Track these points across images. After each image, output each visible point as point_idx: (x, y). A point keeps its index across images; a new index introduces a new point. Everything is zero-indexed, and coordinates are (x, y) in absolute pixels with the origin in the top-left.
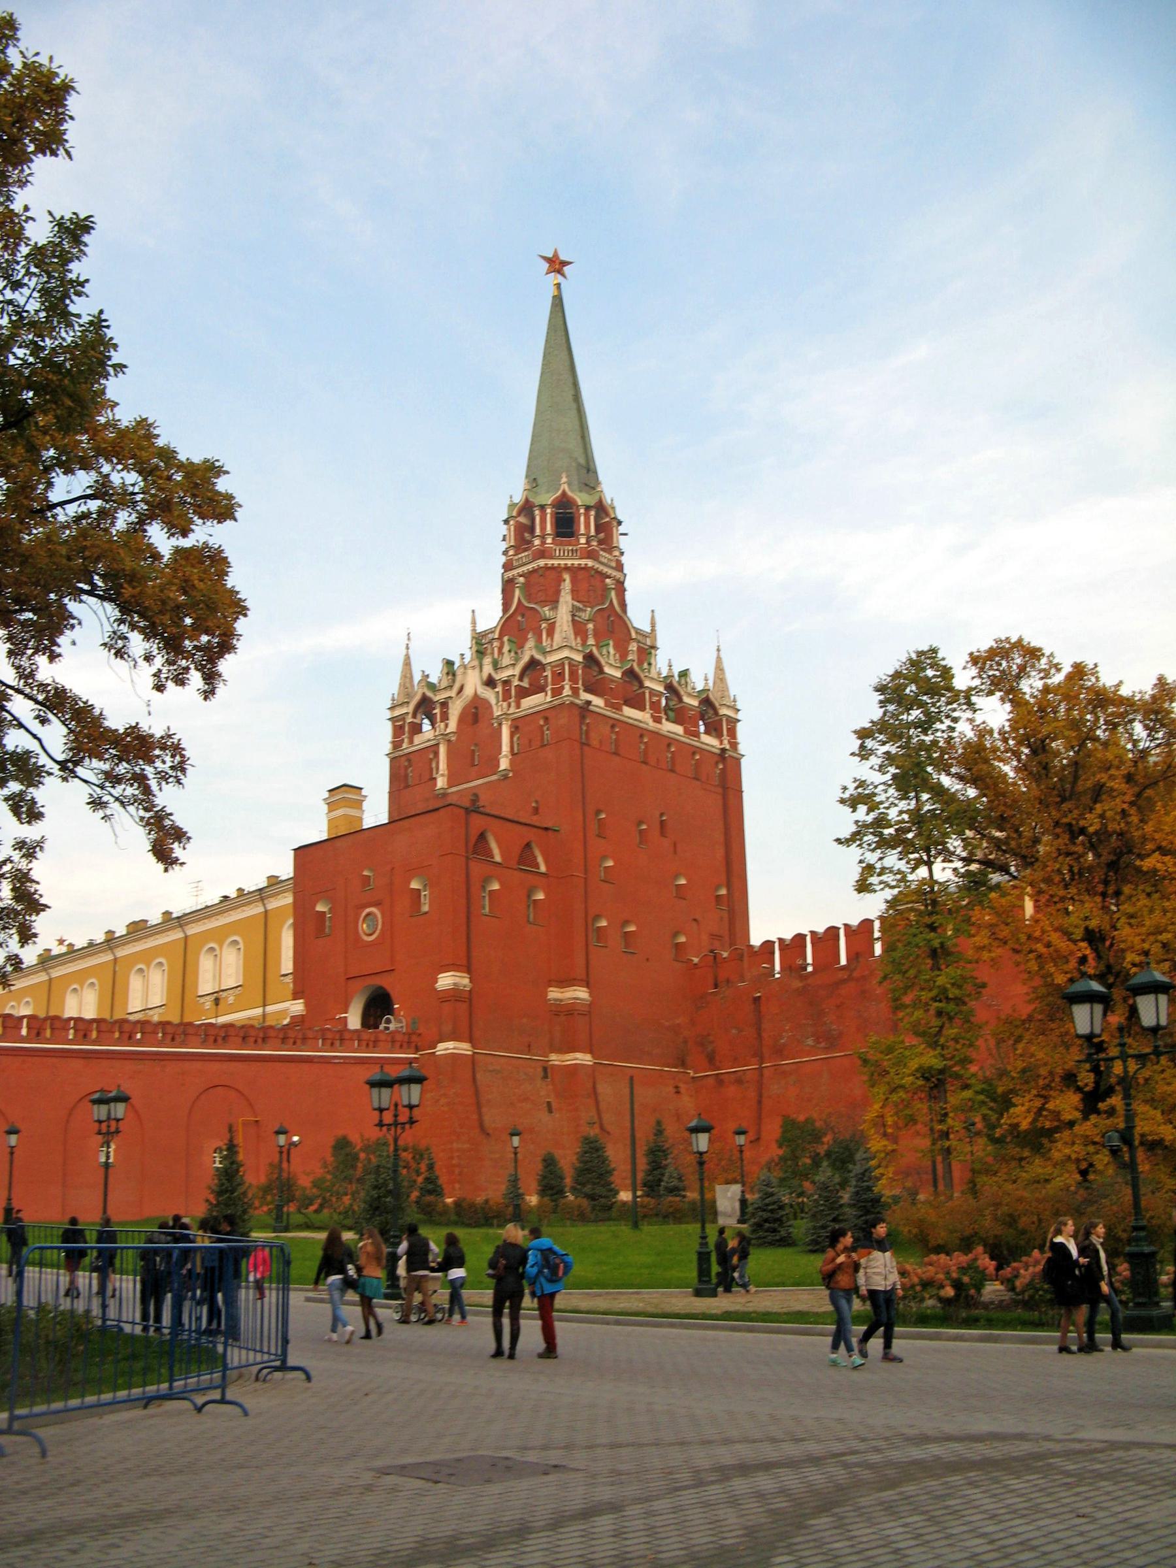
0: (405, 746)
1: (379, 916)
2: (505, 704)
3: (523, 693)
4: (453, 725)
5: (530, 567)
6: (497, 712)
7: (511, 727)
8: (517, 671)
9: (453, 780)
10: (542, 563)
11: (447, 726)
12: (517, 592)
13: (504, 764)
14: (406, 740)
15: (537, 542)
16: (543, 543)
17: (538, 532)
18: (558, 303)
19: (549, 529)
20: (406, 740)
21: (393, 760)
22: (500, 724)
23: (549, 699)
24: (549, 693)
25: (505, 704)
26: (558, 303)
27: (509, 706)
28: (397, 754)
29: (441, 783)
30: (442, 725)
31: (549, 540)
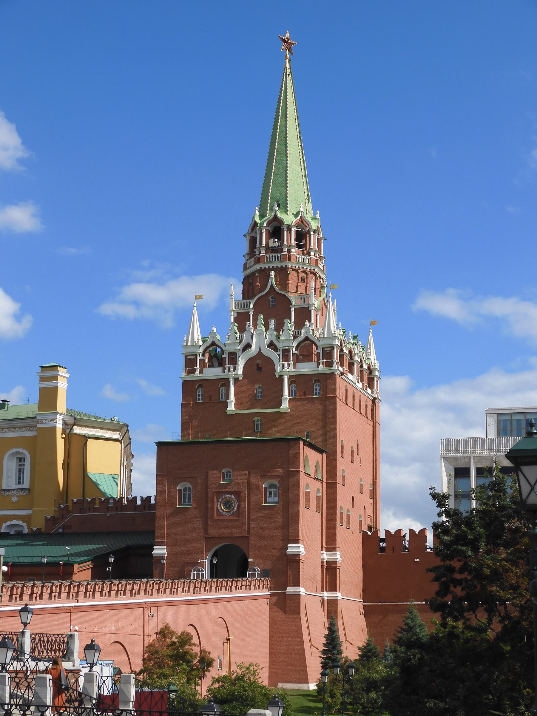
1: (236, 501)
2: (286, 364)
3: (297, 360)
4: (240, 371)
6: (279, 368)
7: (288, 379)
8: (295, 344)
9: (238, 405)
11: (235, 369)
15: (285, 250)
16: (289, 251)
17: (285, 243)
19: (293, 243)
21: (186, 383)
22: (281, 378)
25: (286, 364)
27: (289, 365)
28: (190, 377)
31: (293, 250)
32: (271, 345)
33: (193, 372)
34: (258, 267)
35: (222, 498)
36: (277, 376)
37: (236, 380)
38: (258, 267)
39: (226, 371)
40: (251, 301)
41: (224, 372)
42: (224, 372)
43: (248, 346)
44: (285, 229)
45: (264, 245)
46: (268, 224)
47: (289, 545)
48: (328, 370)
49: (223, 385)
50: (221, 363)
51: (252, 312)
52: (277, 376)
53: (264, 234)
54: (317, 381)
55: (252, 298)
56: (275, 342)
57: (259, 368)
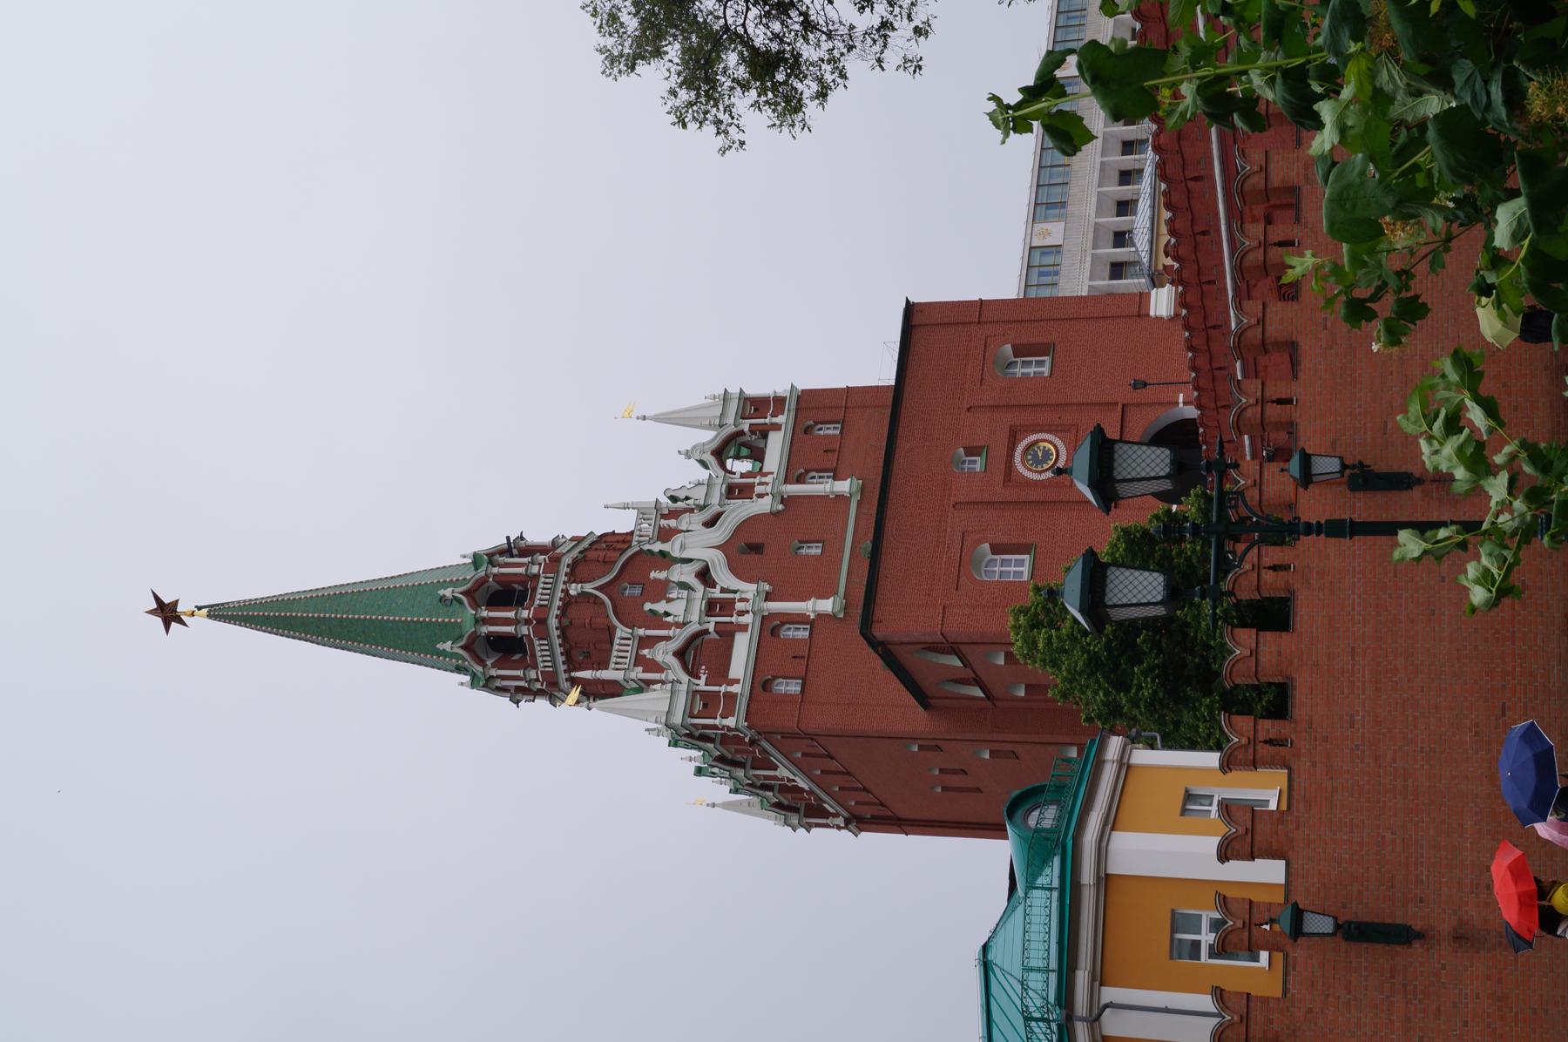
0: (736, 689)
2: (758, 489)
4: (749, 589)
5: (563, 578)
6: (763, 506)
10: (567, 560)
12: (589, 588)
13: (843, 486)
14: (730, 689)
15: (535, 569)
17: (521, 570)
18: (219, 613)
20: (730, 689)
23: (781, 419)
24: (775, 420)
26: (219, 613)
27: (761, 484)
29: (826, 605)
30: (739, 606)
32: (710, 523)
33: (731, 697)
34: (553, 622)
35: (1021, 469)
36: (781, 507)
37: (769, 597)
38: (553, 622)
39: (747, 619)
40: (619, 634)
41: (744, 628)
42: (744, 628)
43: (705, 575)
44: (495, 570)
45: (511, 614)
46: (475, 605)
47: (1152, 313)
48: (791, 405)
49: (774, 632)
50: (727, 634)
51: (641, 632)
52: (781, 507)
53: (492, 614)
54: (807, 430)
55: (611, 631)
56: (707, 515)
57: (756, 548)
